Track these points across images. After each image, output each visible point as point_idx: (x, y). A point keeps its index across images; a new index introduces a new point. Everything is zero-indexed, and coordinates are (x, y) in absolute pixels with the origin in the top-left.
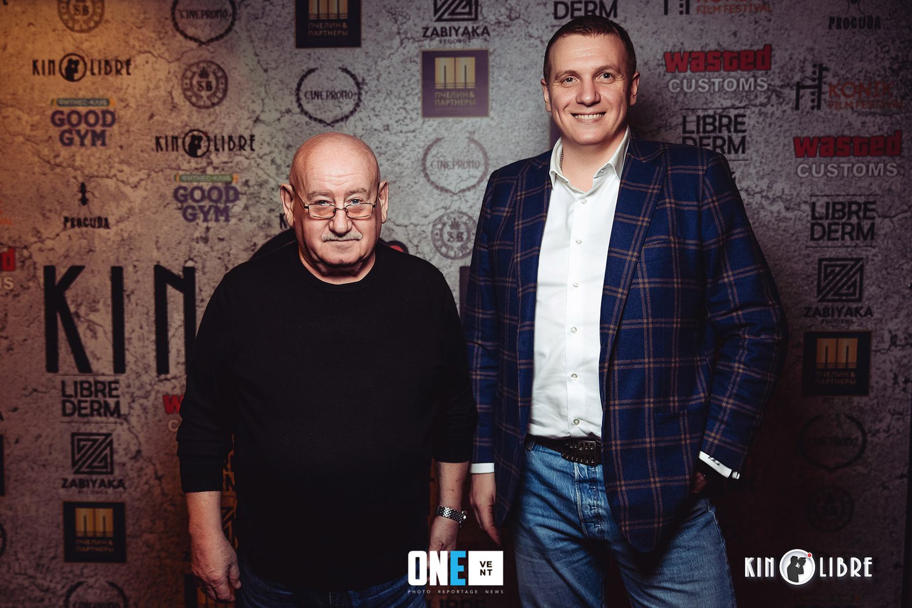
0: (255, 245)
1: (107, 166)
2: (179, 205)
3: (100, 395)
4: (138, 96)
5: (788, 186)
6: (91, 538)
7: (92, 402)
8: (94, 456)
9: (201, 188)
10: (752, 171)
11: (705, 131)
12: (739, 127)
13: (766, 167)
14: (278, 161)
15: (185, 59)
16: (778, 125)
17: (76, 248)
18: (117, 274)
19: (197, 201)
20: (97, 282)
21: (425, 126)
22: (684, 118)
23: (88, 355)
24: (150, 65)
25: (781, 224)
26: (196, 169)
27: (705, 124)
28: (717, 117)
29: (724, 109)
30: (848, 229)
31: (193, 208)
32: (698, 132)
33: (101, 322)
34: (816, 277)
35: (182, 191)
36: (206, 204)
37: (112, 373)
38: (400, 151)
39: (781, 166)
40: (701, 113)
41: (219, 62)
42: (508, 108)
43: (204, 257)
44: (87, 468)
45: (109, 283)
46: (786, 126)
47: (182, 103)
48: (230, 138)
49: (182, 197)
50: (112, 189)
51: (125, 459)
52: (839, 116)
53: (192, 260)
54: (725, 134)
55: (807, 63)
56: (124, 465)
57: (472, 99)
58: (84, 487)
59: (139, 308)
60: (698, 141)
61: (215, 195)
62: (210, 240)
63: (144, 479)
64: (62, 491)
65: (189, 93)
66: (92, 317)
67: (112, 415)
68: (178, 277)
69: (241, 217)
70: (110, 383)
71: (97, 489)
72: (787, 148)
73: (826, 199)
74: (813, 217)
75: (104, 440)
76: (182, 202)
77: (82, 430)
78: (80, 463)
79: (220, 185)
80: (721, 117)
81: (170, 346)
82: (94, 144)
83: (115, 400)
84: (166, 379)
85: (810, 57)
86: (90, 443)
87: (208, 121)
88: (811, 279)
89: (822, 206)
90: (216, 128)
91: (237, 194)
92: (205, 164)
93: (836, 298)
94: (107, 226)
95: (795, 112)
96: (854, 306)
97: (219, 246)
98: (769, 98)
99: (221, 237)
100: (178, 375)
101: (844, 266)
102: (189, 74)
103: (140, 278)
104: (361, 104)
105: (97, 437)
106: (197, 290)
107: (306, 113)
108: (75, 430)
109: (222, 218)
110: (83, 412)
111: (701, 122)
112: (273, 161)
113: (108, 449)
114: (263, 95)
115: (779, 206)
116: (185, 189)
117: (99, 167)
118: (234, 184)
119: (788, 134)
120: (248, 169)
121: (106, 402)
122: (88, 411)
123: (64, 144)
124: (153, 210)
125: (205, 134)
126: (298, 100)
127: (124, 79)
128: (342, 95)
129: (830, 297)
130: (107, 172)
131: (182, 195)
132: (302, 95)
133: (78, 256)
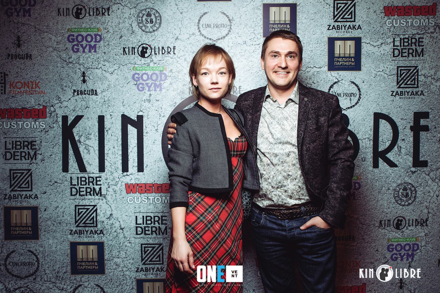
0: (175, 103)
3: (91, 184)
6: (85, 262)
7: (86, 188)
8: (87, 217)
11: (404, 46)
17: (79, 106)
18: (101, 119)
19: (145, 81)
22: (394, 39)
23: (85, 163)
26: (145, 64)
27: (404, 42)
28: (410, 39)
29: (413, 35)
31: (143, 84)
32: (401, 46)
35: (137, 76)
36: (150, 82)
37: (98, 172)
38: (252, 54)
40: (402, 37)
43: (148, 110)
44: (83, 224)
45: (97, 124)
47: (137, 30)
48: (163, 48)
49: (136, 78)
50: (99, 75)
51: (104, 219)
53: (142, 111)
56: (103, 222)
58: (82, 234)
59: (113, 137)
60: (400, 50)
61: (154, 77)
62: (152, 101)
63: (114, 229)
64: (70, 236)
67: (97, 195)
68: (134, 121)
69: (168, 88)
70: (96, 178)
71: (88, 235)
76: (136, 81)
77: (80, 204)
78: (79, 221)
79: (157, 72)
80: (412, 39)
82: (90, 51)
83: (99, 186)
84: (127, 175)
86: (85, 210)
87: (151, 39)
90: (155, 43)
92: (149, 61)
94: (96, 94)
97: (156, 104)
99: (158, 99)
103: (114, 122)
104: (231, 30)
105: (89, 207)
107: (203, 35)
108: (77, 204)
109: (159, 89)
110: (82, 193)
111: (402, 41)
112: (185, 60)
113: (95, 213)
116: (138, 74)
117: (93, 63)
118: (164, 72)
121: (94, 188)
122: (85, 193)
123: (74, 51)
125: (150, 46)
130: (97, 66)
131: (137, 77)
133: (80, 110)
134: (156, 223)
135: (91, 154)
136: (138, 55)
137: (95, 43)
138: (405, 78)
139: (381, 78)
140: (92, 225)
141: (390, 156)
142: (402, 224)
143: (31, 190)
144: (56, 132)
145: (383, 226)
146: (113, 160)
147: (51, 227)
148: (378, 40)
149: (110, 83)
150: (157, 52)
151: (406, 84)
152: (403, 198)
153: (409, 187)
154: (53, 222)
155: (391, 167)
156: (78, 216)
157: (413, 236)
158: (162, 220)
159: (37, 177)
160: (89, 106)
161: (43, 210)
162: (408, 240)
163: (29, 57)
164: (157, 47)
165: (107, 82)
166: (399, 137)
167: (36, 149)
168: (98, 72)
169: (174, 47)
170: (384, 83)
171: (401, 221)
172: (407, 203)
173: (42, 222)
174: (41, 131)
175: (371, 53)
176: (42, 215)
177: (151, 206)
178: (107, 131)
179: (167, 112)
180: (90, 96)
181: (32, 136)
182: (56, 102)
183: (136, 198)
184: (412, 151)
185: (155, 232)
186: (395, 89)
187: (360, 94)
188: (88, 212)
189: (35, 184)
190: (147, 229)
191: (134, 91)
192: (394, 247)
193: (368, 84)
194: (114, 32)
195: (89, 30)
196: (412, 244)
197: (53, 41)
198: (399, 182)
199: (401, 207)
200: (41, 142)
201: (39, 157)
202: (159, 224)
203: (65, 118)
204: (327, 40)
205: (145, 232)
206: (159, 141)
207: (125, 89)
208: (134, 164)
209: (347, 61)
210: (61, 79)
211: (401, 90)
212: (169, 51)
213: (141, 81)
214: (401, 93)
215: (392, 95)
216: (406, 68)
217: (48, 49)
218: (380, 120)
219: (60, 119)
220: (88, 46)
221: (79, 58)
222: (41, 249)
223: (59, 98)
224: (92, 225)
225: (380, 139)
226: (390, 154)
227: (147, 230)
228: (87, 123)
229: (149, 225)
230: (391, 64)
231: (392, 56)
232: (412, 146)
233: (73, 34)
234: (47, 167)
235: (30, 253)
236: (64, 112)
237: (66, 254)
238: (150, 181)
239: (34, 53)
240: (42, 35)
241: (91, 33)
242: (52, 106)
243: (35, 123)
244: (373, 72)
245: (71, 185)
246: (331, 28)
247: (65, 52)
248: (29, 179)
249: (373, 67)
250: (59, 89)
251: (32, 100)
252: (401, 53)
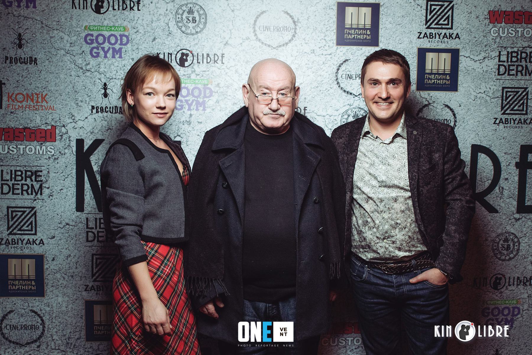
17: (99, 127)
21: (338, 51)
22: (500, 52)
26: (184, 75)
36: (190, 98)
38: (321, 67)
42: (391, 42)
43: (188, 134)
48: (208, 55)
53: (179, 136)
57: (369, 35)
61: (196, 93)
62: (192, 123)
64: (84, 293)
79: (200, 86)
91: (211, 91)
92: (191, 72)
99: (200, 121)
104: (296, 35)
107: (260, 40)
108: (94, 252)
109: (201, 108)
112: (236, 71)
117: (117, 72)
118: (209, 86)
122: (105, 238)
133: (100, 133)
139: (482, 101)
141: (490, 198)
143: (35, 234)
144: (68, 160)
147: (61, 281)
148: (480, 54)
154: (63, 275)
155: (490, 212)
156: (96, 268)
159: (43, 217)
161: (50, 259)
163: (33, 61)
167: (41, 181)
170: (486, 107)
173: (49, 274)
174: (49, 158)
175: (470, 70)
176: (49, 266)
181: (36, 164)
182: (69, 121)
186: (499, 116)
187: (455, 121)
189: (40, 226)
192: (490, 311)
193: (466, 109)
197: (65, 41)
198: (499, 231)
200: (48, 172)
201: (46, 192)
203: (80, 142)
204: (416, 51)
209: (440, 79)
210: (76, 91)
212: (216, 59)
215: (494, 123)
217: (59, 52)
218: (479, 154)
219: (74, 144)
221: (99, 64)
222: (48, 309)
223: (73, 116)
225: (478, 178)
226: (489, 196)
230: (495, 83)
231: (497, 74)
233: (91, 33)
234: (56, 204)
235: (33, 314)
236: (79, 134)
237: (80, 316)
239: (40, 56)
240: (51, 32)
242: (64, 126)
243: (41, 148)
244: (473, 93)
245: (87, 228)
246: (422, 36)
247: (81, 56)
248: (33, 219)
250: (73, 104)
251: (38, 117)
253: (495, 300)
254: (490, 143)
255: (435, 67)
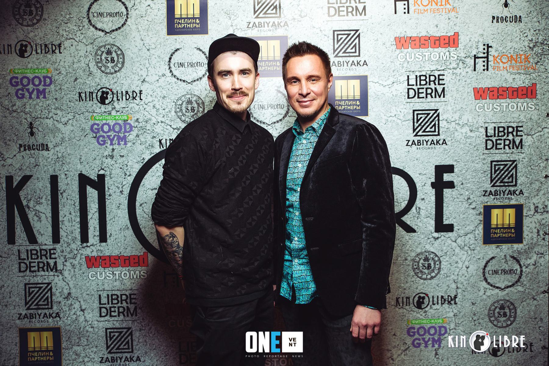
0: (144, 159)
1: (46, 111)
2: (95, 135)
3: (44, 258)
4: (67, 67)
5: (471, 117)
7: (38, 262)
8: (40, 298)
9: (108, 124)
10: (450, 108)
12: (441, 82)
13: (457, 106)
14: (158, 107)
15: (96, 43)
16: (464, 80)
19: (106, 132)
20: (40, 186)
22: (408, 76)
23: (35, 233)
24: (74, 47)
25: (467, 140)
26: (105, 112)
27: (420, 80)
28: (428, 76)
30: (507, 142)
31: (103, 137)
32: (417, 85)
33: (43, 211)
34: (490, 172)
35: (96, 126)
36: (112, 134)
37: (51, 243)
39: (466, 105)
40: (418, 74)
41: (118, 45)
43: (111, 167)
44: (35, 305)
45: (49, 186)
46: (469, 81)
47: (96, 71)
48: (127, 93)
50: (50, 126)
51: (60, 299)
52: (499, 75)
53: (103, 169)
54: (432, 86)
55: (480, 43)
56: (60, 303)
58: (33, 318)
59: (69, 201)
61: (117, 128)
63: (73, 311)
65: (100, 65)
66: (38, 208)
67: (52, 270)
69: (134, 142)
70: (50, 250)
72: (469, 94)
73: (494, 125)
74: (487, 136)
75: (47, 287)
76: (96, 133)
79: (120, 122)
80: (430, 76)
81: (89, 225)
82: (38, 97)
83: (54, 260)
84: (87, 246)
85: (481, 40)
88: (486, 173)
89: (491, 129)
91: (131, 127)
92: (111, 109)
93: (502, 184)
94: (47, 149)
95: (474, 72)
96: (512, 189)
97: (120, 160)
98: (458, 64)
99: (122, 154)
100: (95, 243)
101: (506, 165)
102: (99, 53)
103: (69, 182)
105: (42, 285)
106: (106, 189)
107: (175, 76)
109: (123, 143)
111: (418, 79)
112: (154, 106)
113: (49, 292)
114: (147, 65)
115: (466, 129)
116: (98, 125)
117: (42, 112)
119: (470, 86)
120: (138, 112)
121: (47, 262)
122: (36, 268)
124: (77, 138)
125: (111, 90)
126: (170, 68)
127: (58, 56)
128: (197, 64)
129: (498, 184)
131: (96, 129)
132: (172, 65)
134: (124, 302)
135: (43, 222)
136: (96, 102)
137: (44, 87)
138: (422, 124)
140: (46, 307)
141: (406, 219)
142: (425, 302)
145: (401, 305)
146: (70, 229)
148: (388, 79)
149: (64, 135)
150: (120, 98)
151: (424, 131)
152: (424, 271)
153: (432, 256)
155: (408, 232)
157: (439, 317)
158: (131, 299)
160: (38, 164)
162: (433, 321)
164: (120, 92)
165: (60, 135)
166: (418, 196)
168: (48, 123)
169: (141, 91)
171: (424, 298)
172: (429, 277)
177: (117, 282)
178: (61, 194)
179: (134, 170)
180: (40, 152)
183: (98, 273)
184: (434, 213)
185: (123, 313)
186: (412, 137)
188: (40, 291)
190: (113, 309)
191: (93, 145)
192: (416, 330)
194: (67, 73)
195: (36, 71)
196: (439, 327)
198: (419, 250)
199: (422, 281)
202: (127, 303)
205: (110, 314)
206: (124, 205)
207: (82, 143)
208: (95, 233)
209: (350, 105)
211: (419, 138)
212: (134, 96)
213: (101, 133)
214: (418, 143)
216: (424, 112)
218: (393, 176)
220: (35, 91)
224: (46, 307)
226: (406, 216)
227: (113, 311)
228: (37, 185)
229: (115, 305)
230: (405, 107)
232: (434, 206)
238: (116, 253)
241: (39, 75)
244: (384, 117)
249: (383, 111)
252: (418, 94)
253: (420, 319)
254: (404, 164)
255: (344, 94)
